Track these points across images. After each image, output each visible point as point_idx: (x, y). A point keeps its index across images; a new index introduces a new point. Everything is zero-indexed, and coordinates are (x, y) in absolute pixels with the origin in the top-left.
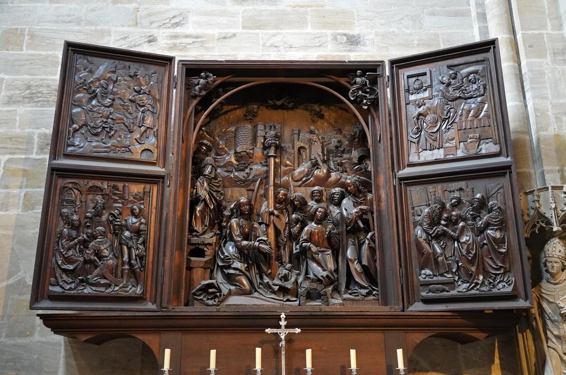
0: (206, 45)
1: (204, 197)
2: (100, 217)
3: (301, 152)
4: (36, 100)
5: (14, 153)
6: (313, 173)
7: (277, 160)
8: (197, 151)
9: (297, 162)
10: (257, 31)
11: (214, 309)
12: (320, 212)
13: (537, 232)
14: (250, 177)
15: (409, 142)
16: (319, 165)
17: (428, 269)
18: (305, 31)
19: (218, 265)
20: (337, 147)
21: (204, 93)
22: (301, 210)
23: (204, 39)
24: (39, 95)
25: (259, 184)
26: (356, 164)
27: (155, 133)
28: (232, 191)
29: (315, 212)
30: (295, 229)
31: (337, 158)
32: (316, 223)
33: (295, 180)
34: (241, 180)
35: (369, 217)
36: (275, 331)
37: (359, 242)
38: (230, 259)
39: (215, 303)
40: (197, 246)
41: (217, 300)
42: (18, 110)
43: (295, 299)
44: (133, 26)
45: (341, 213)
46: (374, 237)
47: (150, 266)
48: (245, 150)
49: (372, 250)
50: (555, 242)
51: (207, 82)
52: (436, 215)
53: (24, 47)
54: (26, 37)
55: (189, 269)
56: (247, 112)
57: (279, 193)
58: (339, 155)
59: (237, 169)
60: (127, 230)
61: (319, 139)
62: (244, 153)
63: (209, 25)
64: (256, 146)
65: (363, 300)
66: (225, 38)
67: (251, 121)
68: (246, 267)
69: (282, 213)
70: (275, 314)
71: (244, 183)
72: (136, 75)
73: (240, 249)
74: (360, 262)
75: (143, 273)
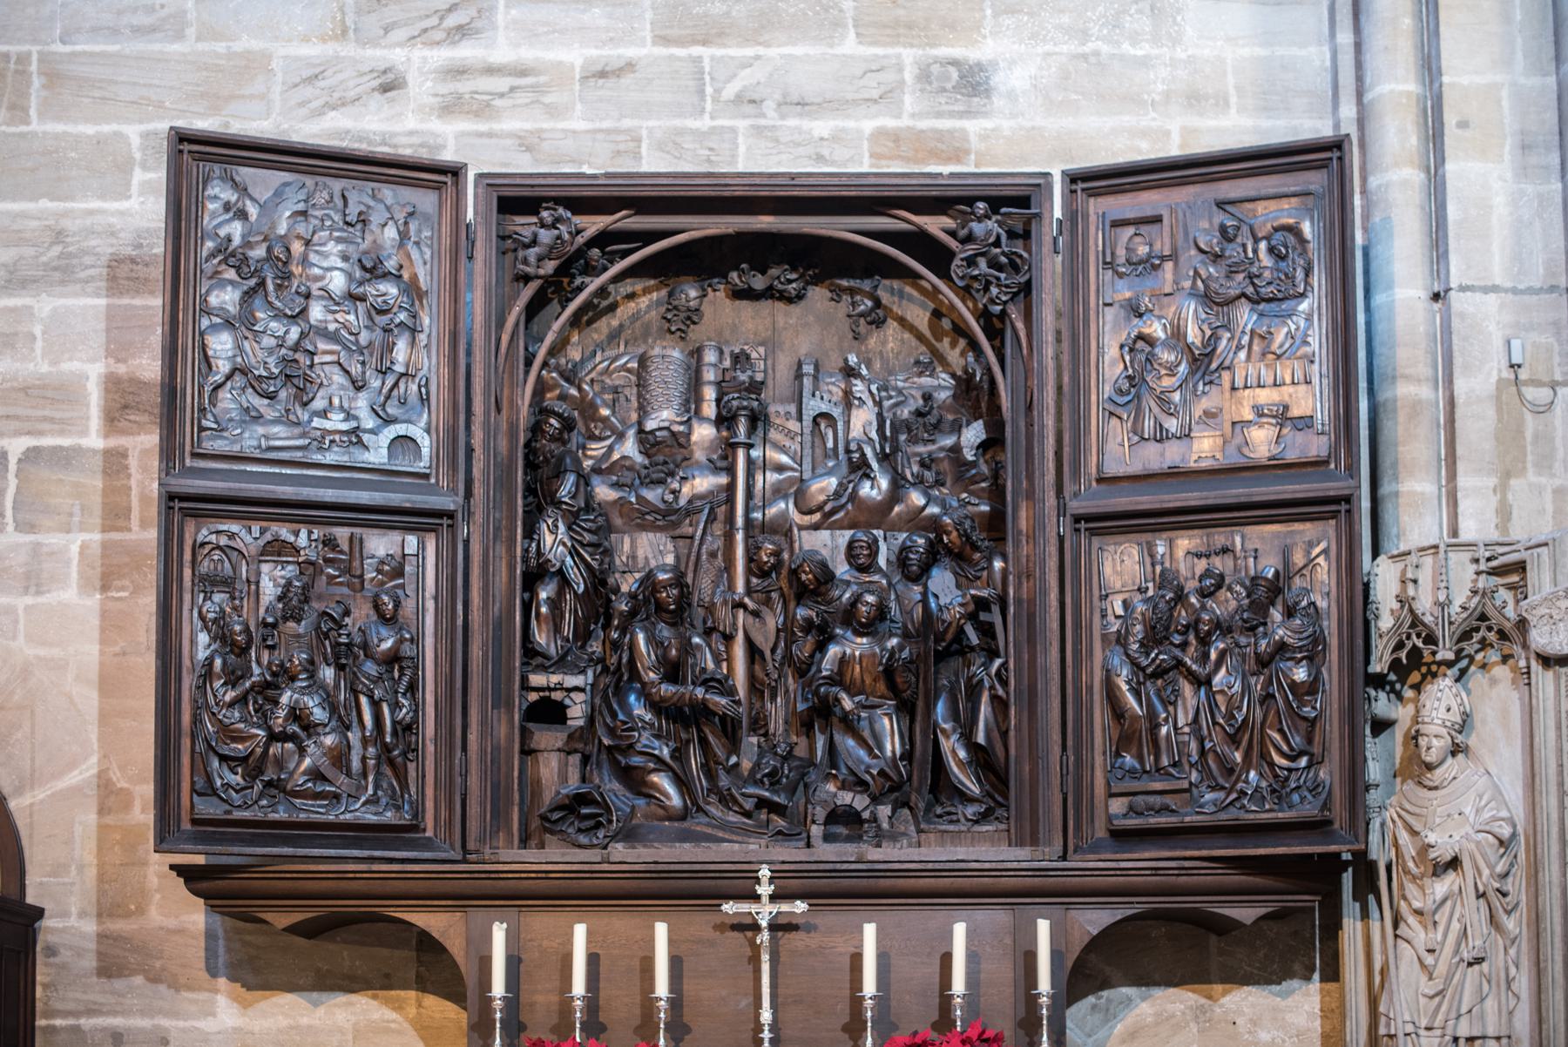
0: (547, 99)
1: (558, 564)
3: (823, 426)
4: (83, 275)
5: (41, 433)
7: (755, 453)
8: (536, 429)
9: (809, 459)
10: (696, 50)
11: (593, 855)
13: (1405, 661)
15: (1107, 414)
16: (869, 466)
18: (838, 50)
19: (600, 741)
20: (919, 413)
21: (550, 267)
22: (819, 595)
23: (542, 79)
24: (88, 260)
25: (706, 523)
27: (423, 390)
30: (803, 649)
31: (921, 449)
33: (804, 510)
34: (656, 511)
39: (595, 842)
40: (547, 694)
41: (601, 834)
42: (36, 306)
44: (335, 38)
46: (1006, 670)
47: (431, 748)
48: (666, 424)
49: (1000, 704)
53: (33, 112)
54: (36, 82)
55: (527, 752)
56: (668, 310)
61: (870, 391)
62: (665, 433)
63: (554, 32)
64: (698, 412)
65: (969, 831)
66: (603, 74)
69: (768, 602)
70: (745, 867)
73: (656, 706)
75: (414, 764)
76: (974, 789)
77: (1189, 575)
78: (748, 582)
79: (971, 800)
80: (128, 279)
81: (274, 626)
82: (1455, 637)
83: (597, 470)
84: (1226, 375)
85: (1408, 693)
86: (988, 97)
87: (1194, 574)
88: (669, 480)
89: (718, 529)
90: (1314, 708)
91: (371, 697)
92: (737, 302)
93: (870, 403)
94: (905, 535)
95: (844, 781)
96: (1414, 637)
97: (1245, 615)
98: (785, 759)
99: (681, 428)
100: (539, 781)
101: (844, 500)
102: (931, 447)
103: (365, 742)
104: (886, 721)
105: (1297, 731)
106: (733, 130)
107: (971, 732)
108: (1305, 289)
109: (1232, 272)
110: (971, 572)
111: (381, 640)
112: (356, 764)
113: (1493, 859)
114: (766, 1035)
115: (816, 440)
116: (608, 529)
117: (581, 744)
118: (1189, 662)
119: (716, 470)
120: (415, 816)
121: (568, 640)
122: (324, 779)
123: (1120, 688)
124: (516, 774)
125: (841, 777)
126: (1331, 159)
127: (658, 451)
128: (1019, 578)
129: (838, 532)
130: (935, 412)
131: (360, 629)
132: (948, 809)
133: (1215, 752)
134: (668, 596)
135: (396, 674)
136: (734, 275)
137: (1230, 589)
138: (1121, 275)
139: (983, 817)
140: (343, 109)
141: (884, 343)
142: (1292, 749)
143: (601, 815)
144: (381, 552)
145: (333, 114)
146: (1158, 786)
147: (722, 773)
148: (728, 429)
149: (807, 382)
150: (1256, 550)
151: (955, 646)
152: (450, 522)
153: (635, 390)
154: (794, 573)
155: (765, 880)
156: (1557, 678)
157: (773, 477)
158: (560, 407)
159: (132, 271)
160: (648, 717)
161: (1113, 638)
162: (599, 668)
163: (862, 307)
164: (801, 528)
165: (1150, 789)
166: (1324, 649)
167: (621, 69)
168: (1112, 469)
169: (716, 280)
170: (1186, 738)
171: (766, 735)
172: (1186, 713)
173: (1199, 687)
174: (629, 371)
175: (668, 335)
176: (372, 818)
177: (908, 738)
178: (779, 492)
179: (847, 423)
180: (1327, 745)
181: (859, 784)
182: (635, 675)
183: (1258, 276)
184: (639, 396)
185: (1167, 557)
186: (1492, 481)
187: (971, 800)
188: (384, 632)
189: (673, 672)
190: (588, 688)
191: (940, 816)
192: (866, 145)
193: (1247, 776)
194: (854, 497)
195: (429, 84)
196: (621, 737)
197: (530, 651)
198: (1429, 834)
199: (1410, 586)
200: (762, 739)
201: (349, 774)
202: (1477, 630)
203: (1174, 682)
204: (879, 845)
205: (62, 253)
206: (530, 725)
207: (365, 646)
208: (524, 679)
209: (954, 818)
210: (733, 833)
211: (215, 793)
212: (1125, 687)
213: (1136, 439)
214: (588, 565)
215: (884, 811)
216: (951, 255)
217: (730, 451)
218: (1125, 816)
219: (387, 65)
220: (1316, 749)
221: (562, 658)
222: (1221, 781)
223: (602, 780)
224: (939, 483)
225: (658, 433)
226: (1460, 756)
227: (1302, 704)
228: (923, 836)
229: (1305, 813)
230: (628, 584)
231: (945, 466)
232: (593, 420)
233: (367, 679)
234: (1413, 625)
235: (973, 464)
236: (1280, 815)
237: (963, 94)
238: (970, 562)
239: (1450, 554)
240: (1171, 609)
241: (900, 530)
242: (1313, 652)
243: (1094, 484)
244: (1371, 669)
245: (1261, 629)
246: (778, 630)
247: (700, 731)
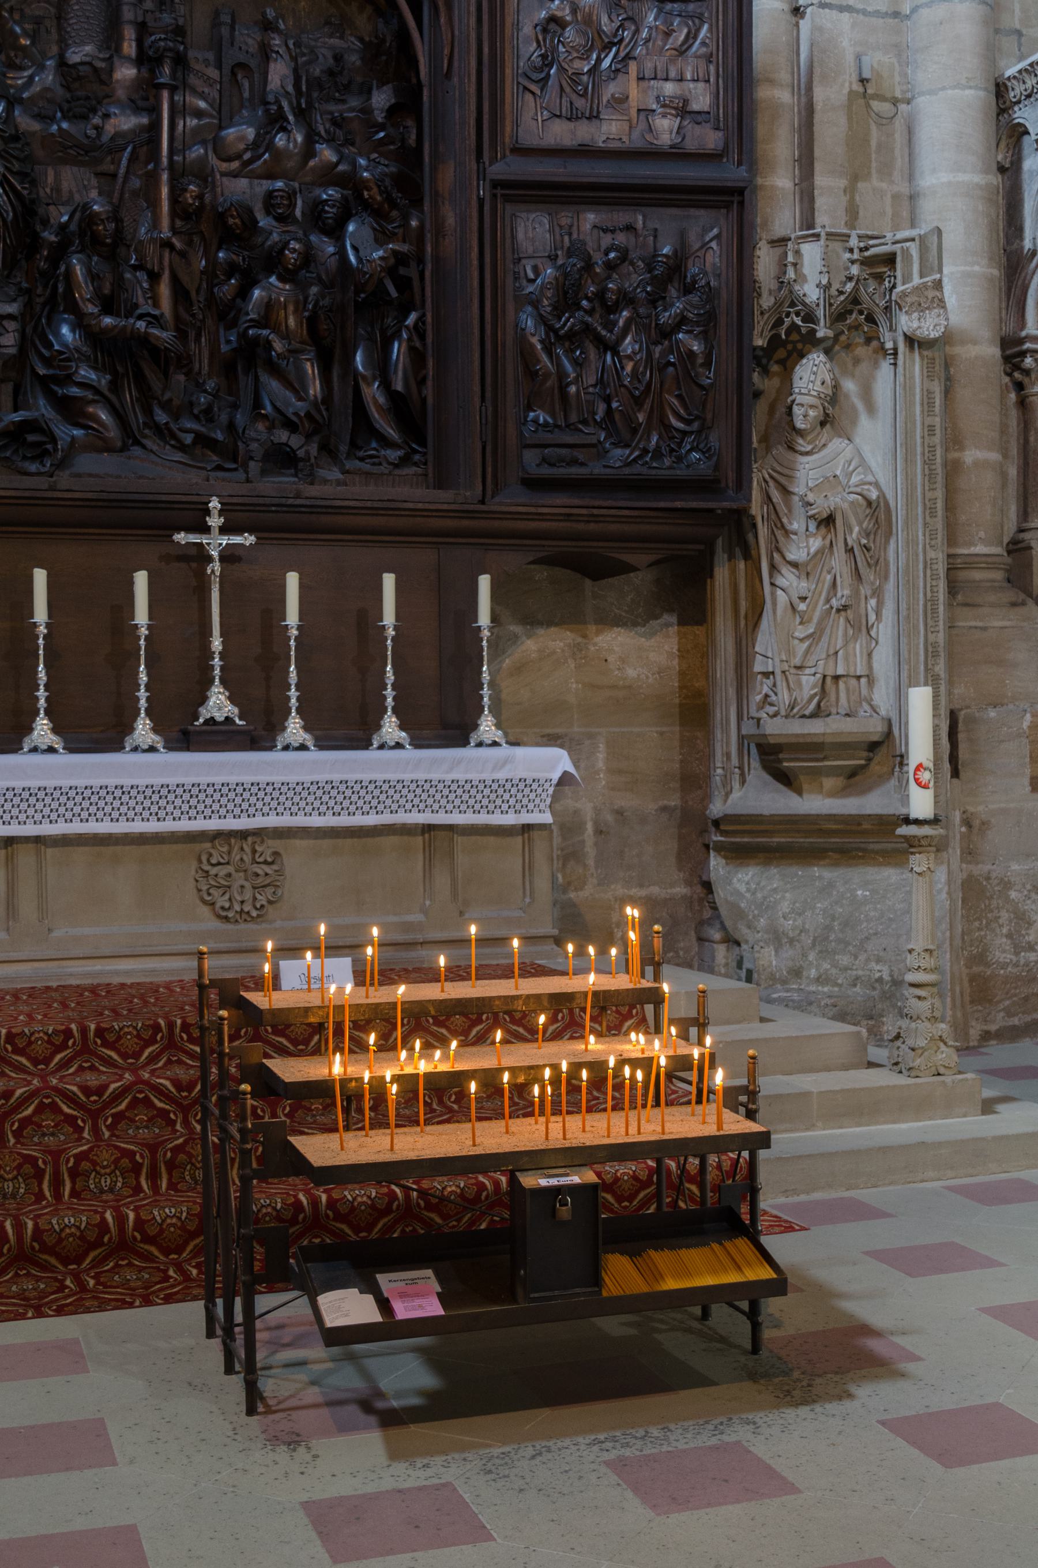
3: (239, 77)
6: (272, 141)
11: (43, 482)
12: (294, 250)
13: (783, 337)
14: (105, 138)
15: (521, 88)
16: (287, 120)
17: (543, 410)
19: (33, 370)
20: (331, 73)
25: (130, 160)
26: (382, 127)
28: (56, 173)
29: (281, 251)
31: (332, 107)
32: (281, 279)
35: (412, 272)
36: (194, 538)
37: (383, 331)
38: (68, 360)
39: (43, 470)
43: (234, 466)
45: (342, 254)
46: (424, 323)
48: (88, 59)
49: (417, 357)
50: (816, 362)
52: (573, 285)
57: (186, 190)
59: (69, 110)
62: (86, 68)
64: (118, 49)
65: (390, 474)
70: (195, 499)
71: (87, 152)
73: (93, 336)
74: (386, 385)
76: (391, 433)
77: (595, 247)
85: (775, 368)
87: (599, 246)
88: (91, 116)
93: (287, 57)
99: (103, 65)
102: (340, 107)
104: (308, 366)
119: (137, 110)
123: (532, 346)
129: (256, 181)
134: (105, 229)
139: (405, 461)
143: (45, 443)
157: (192, 122)
164: (223, 174)
178: (197, 136)
181: (291, 426)
186: (843, 183)
194: (270, 147)
202: (851, 312)
204: (312, 484)
209: (376, 460)
225: (81, 68)
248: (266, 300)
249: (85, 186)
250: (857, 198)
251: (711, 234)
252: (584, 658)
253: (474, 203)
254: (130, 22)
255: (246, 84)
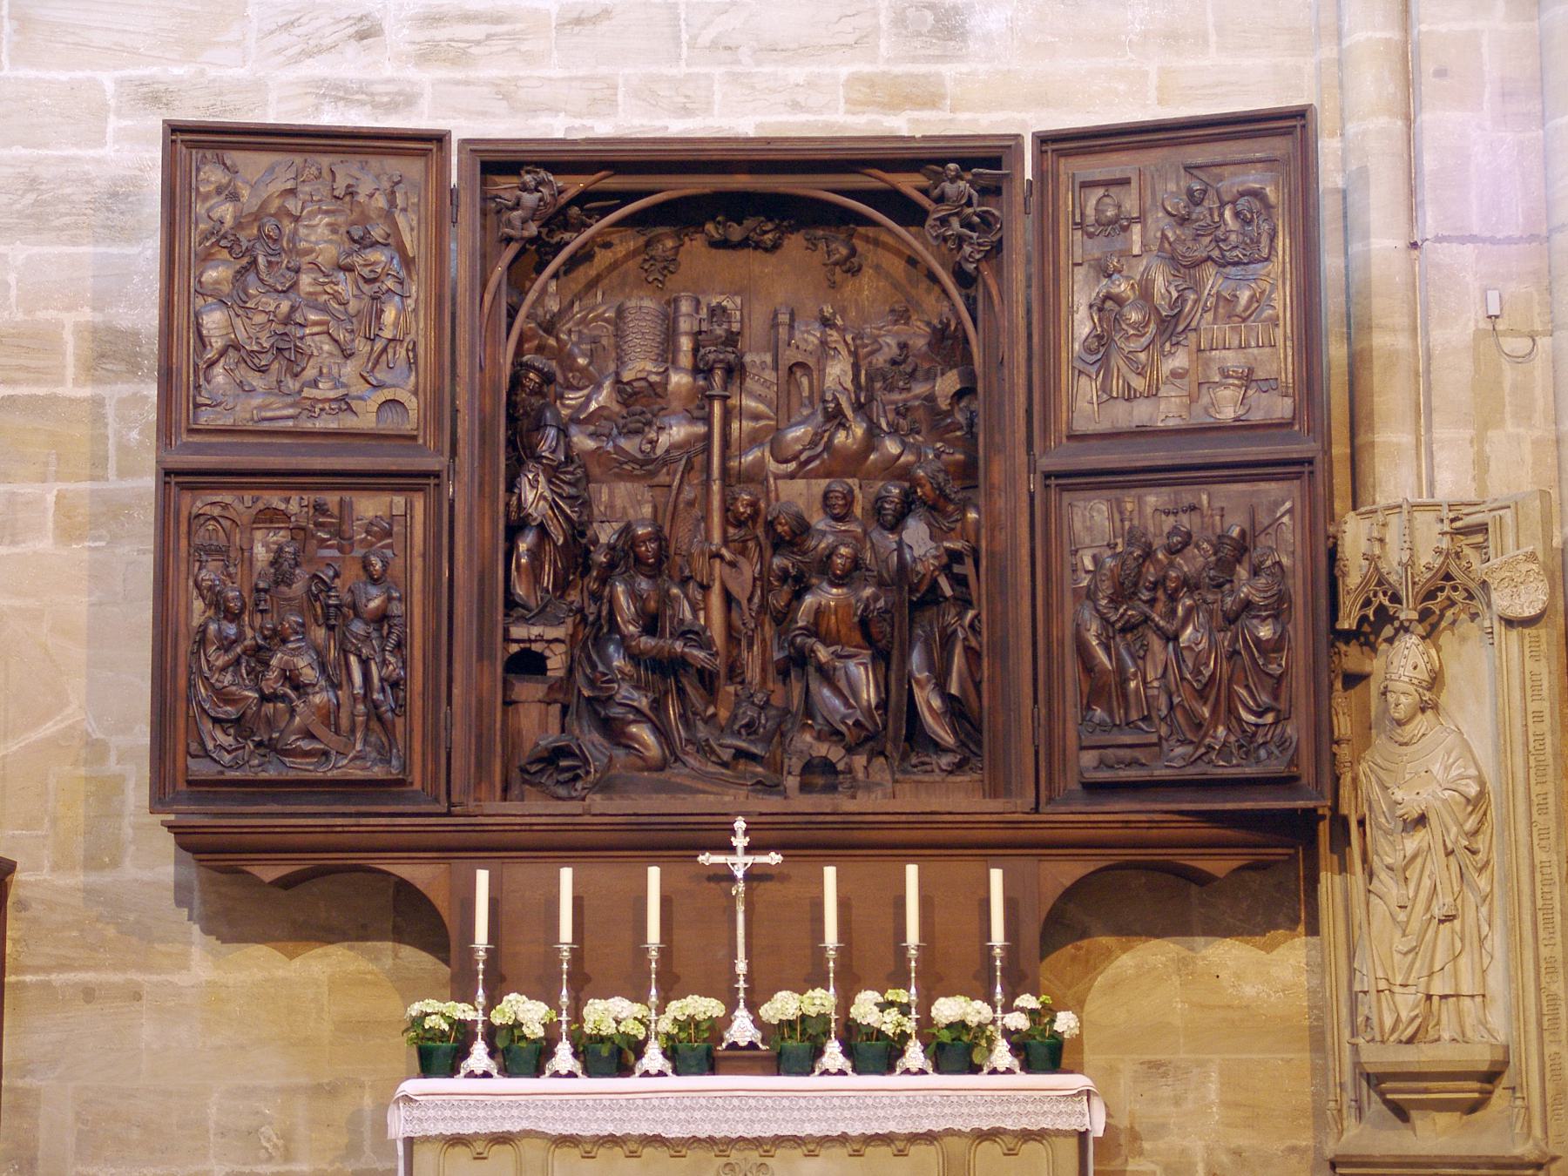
0: (524, 47)
1: (539, 520)
2: (289, 585)
3: (798, 374)
4: (56, 223)
6: (831, 439)
8: (516, 382)
12: (843, 556)
14: (659, 452)
15: (1076, 373)
16: (845, 416)
19: (579, 691)
20: (894, 362)
22: (796, 545)
23: (519, 26)
24: (62, 208)
25: (683, 473)
29: (829, 557)
30: (779, 600)
31: (896, 396)
34: (634, 460)
35: (967, 569)
37: (943, 630)
40: (528, 645)
41: (579, 785)
46: (979, 621)
47: (418, 703)
48: (643, 375)
49: (973, 655)
51: (541, 199)
55: (508, 703)
57: (736, 499)
58: (901, 384)
59: (623, 427)
60: (357, 615)
62: (643, 384)
64: (674, 362)
65: (943, 781)
66: (578, 21)
67: (658, 286)
68: (655, 701)
69: (743, 552)
72: (352, 194)
73: (634, 657)
74: (941, 686)
75: (402, 719)
76: (948, 739)
78: (725, 532)
79: (946, 750)
80: (103, 227)
81: (266, 591)
82: (1420, 597)
83: (574, 420)
84: (1192, 336)
86: (964, 41)
88: (647, 429)
89: (696, 478)
90: (1280, 665)
91: (359, 656)
92: (714, 251)
93: (844, 352)
94: (881, 484)
95: (820, 732)
96: (1381, 594)
97: (1212, 573)
98: (762, 708)
100: (519, 732)
101: (820, 449)
102: (904, 395)
103: (355, 698)
105: (1263, 687)
106: (708, 76)
107: (946, 680)
108: (1270, 254)
109: (1199, 235)
110: (946, 524)
111: (369, 600)
112: (344, 722)
113: (1461, 817)
114: (742, 984)
115: (792, 388)
116: (588, 478)
117: (563, 696)
118: (1157, 619)
119: (693, 420)
120: (404, 768)
121: (547, 591)
122: (310, 736)
124: (498, 725)
125: (817, 727)
126: (1295, 126)
127: (636, 400)
128: (992, 530)
129: (813, 481)
130: (910, 360)
131: (350, 590)
132: (923, 759)
133: (1183, 707)
134: (647, 550)
135: (385, 632)
136: (710, 227)
137: (1197, 546)
138: (1091, 236)
139: (958, 767)
140: (319, 57)
141: (860, 291)
142: (1259, 706)
143: (579, 767)
144: (370, 514)
145: (309, 61)
146: (1128, 740)
147: (700, 725)
148: (705, 379)
149: (783, 332)
150: (1222, 509)
151: (928, 598)
152: (436, 481)
153: (612, 340)
154: (770, 525)
155: (740, 833)
156: (1522, 638)
157: (748, 425)
158: (539, 361)
159: (108, 219)
160: (628, 669)
161: (1084, 592)
162: (578, 617)
163: (837, 256)
164: (777, 477)
165: (1120, 742)
166: (1290, 607)
167: (598, 16)
168: (1081, 426)
169: (692, 229)
170: (1156, 692)
171: (742, 683)
172: (1155, 668)
173: (1167, 642)
174: (607, 320)
175: (645, 284)
176: (359, 774)
177: (884, 686)
178: (754, 440)
179: (822, 371)
180: (1294, 700)
181: (834, 734)
182: (614, 626)
183: (1224, 240)
184: (618, 347)
185: (1136, 513)
186: (1468, 433)
187: (946, 750)
188: (373, 591)
189: (651, 625)
190: (568, 641)
191: (915, 766)
192: (841, 92)
193: (1215, 731)
194: (829, 446)
195: (406, 31)
196: (601, 689)
197: (511, 603)
198: (1396, 791)
199: (1377, 544)
200: (739, 687)
201: (337, 732)
203: (1143, 636)
204: (854, 797)
205: (36, 201)
206: (511, 677)
207: (354, 606)
208: (506, 631)
209: (928, 768)
210: (714, 784)
211: (207, 754)
212: (1095, 643)
213: (1105, 397)
214: (567, 518)
215: (860, 761)
216: (925, 213)
217: (706, 402)
218: (1096, 768)
219: (364, 13)
220: (1283, 706)
221: (542, 611)
222: (1190, 736)
223: (582, 731)
224: (914, 431)
225: (635, 384)
226: (1429, 713)
227: (1268, 661)
228: (898, 786)
229: (1272, 768)
230: (606, 534)
231: (920, 414)
232: (571, 371)
233: (356, 638)
234: (1380, 583)
235: (949, 413)
236: (1247, 770)
237: (938, 38)
238: (946, 516)
239: (1415, 514)
240: (1140, 566)
241: (875, 478)
242: (1278, 609)
243: (1064, 440)
244: (1339, 626)
245: (1227, 586)
246: (755, 579)
247: (677, 681)
248: (815, 606)
249: (639, 502)
250: (1487, 448)
251: (1283, 509)
252: (1192, 974)
253: (1025, 498)
254: (686, 333)
255: (805, 381)
